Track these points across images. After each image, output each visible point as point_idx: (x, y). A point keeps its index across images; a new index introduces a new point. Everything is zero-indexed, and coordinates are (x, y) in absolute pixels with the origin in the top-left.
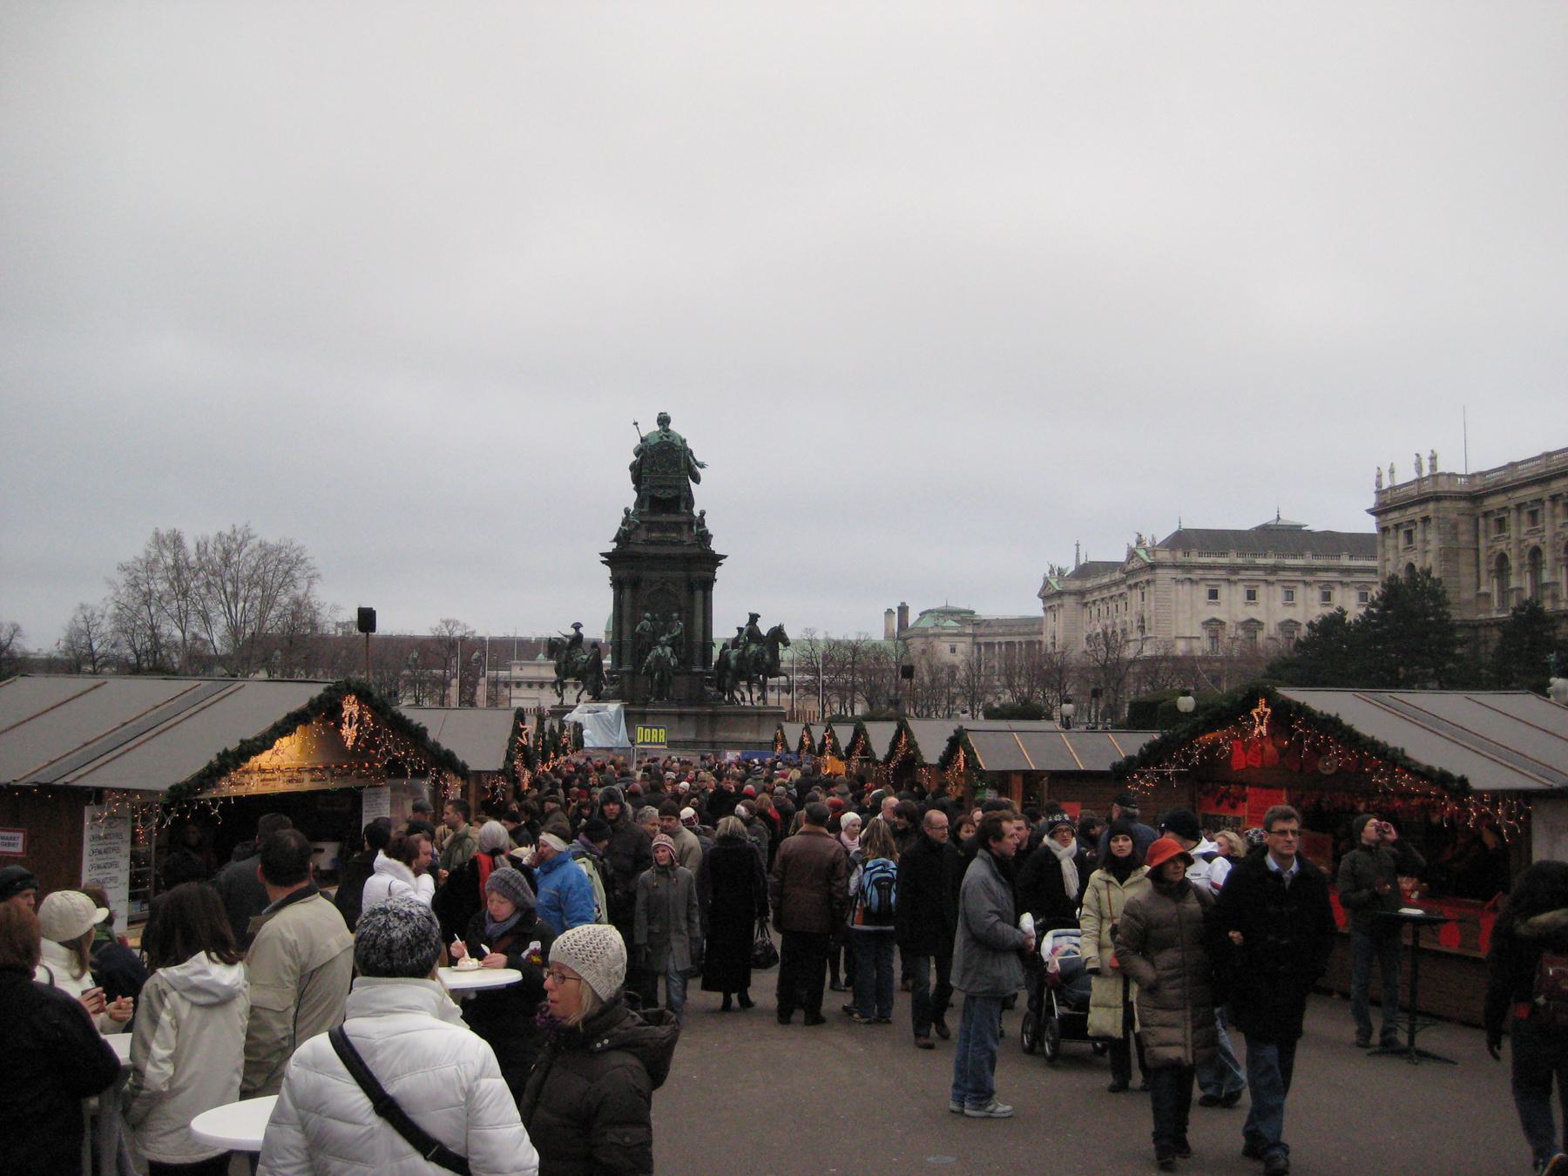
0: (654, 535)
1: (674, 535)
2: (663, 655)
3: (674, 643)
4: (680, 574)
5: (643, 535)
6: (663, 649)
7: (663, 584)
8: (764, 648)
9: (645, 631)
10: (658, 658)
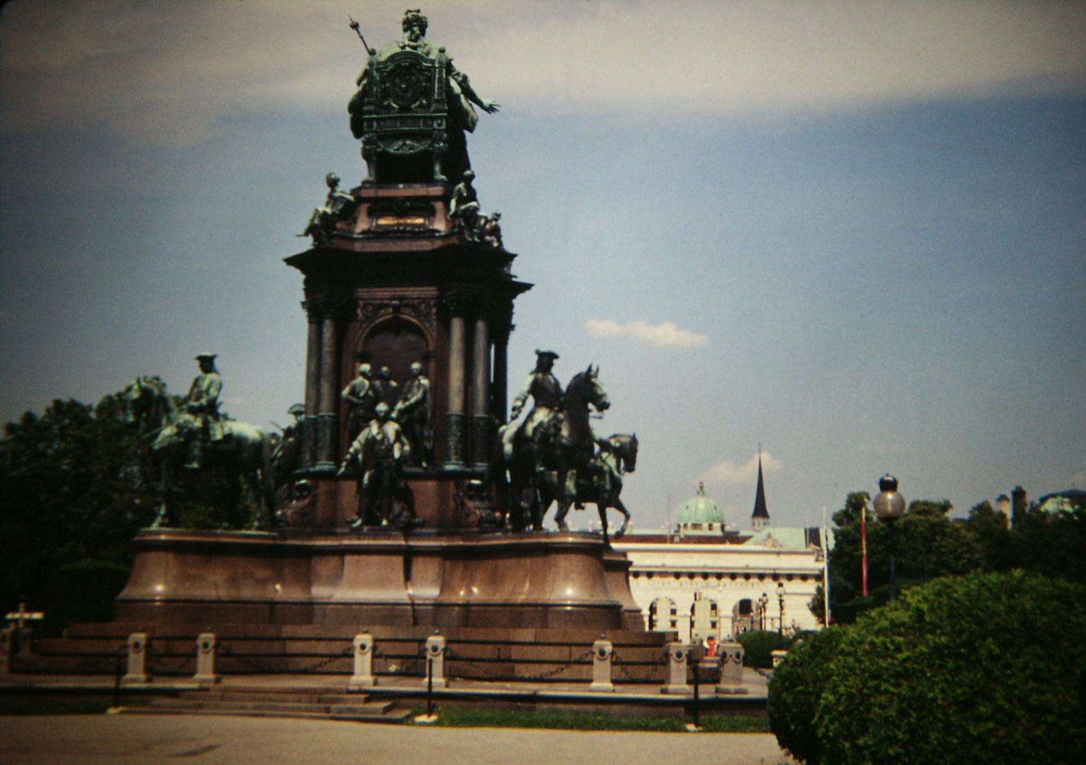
0: (382, 222)
1: (420, 221)
2: (379, 437)
3: (410, 423)
4: (431, 291)
5: (363, 225)
6: (380, 427)
7: (396, 309)
8: (561, 416)
9: (358, 397)
10: (371, 443)
